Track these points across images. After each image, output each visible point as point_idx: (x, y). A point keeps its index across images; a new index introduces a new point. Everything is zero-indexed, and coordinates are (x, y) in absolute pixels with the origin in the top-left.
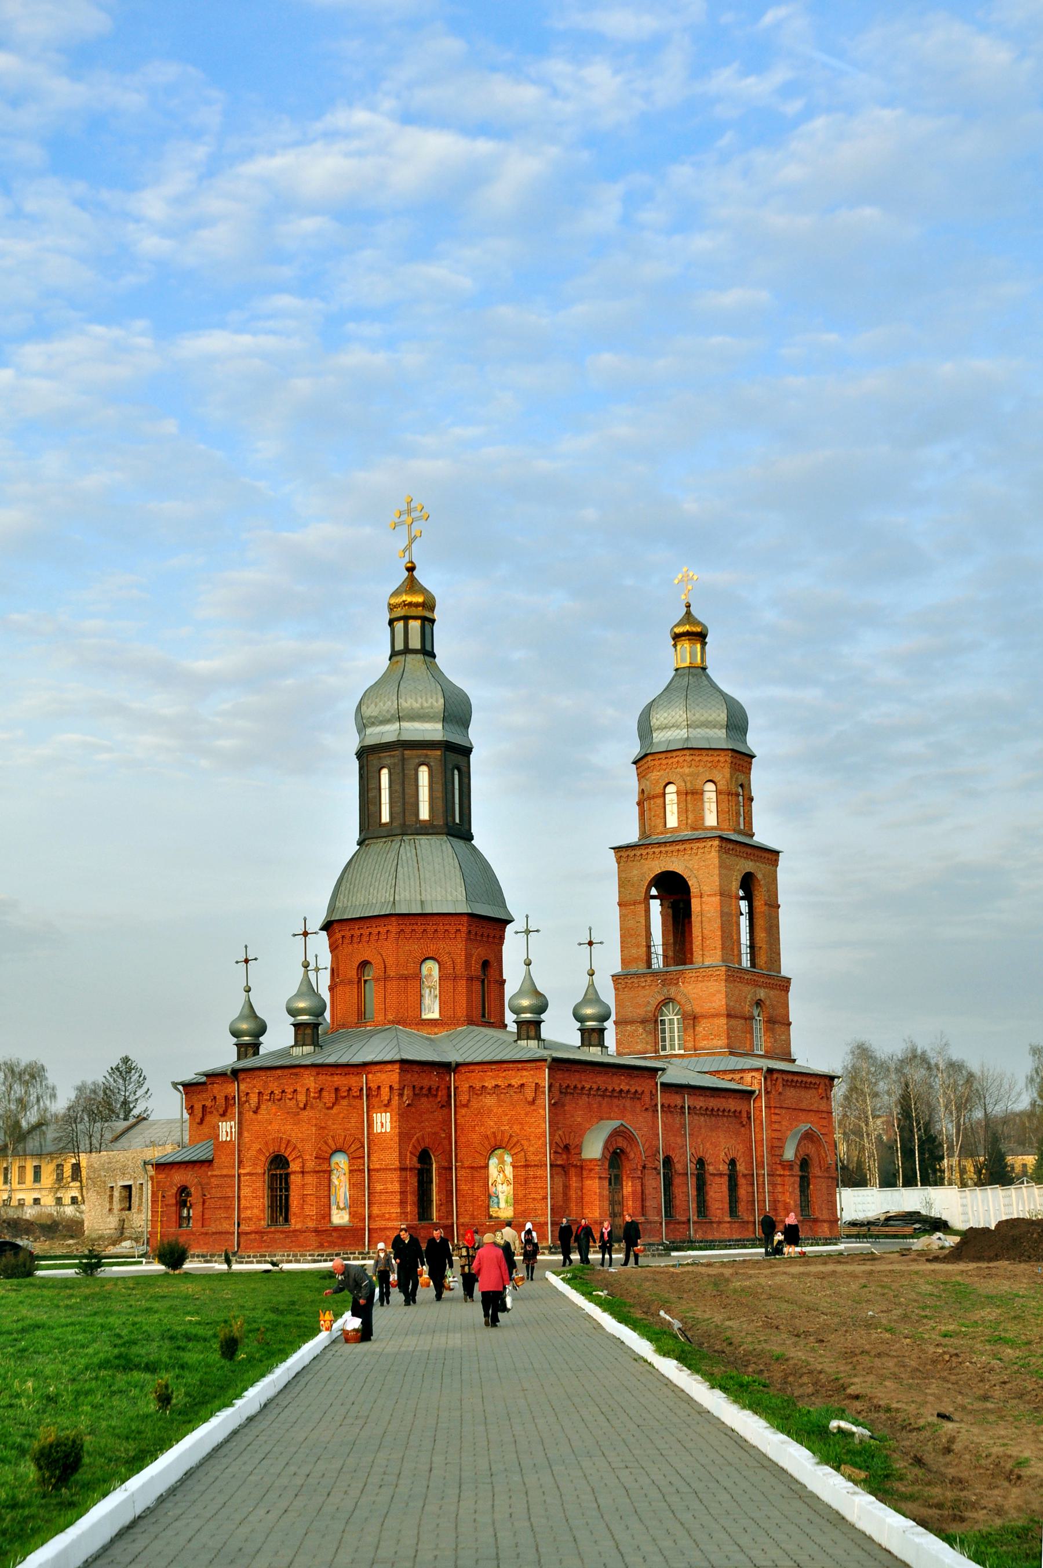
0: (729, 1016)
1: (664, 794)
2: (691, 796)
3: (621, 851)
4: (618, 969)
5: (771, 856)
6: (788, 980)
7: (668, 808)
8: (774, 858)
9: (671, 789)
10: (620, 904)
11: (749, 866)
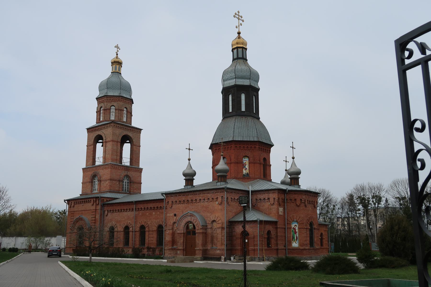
0: (111, 180)
1: (100, 111)
2: (107, 111)
3: (89, 130)
4: (84, 166)
5: (139, 130)
6: (142, 169)
7: (101, 114)
8: (139, 131)
9: (102, 109)
10: (87, 146)
11: (125, 133)
